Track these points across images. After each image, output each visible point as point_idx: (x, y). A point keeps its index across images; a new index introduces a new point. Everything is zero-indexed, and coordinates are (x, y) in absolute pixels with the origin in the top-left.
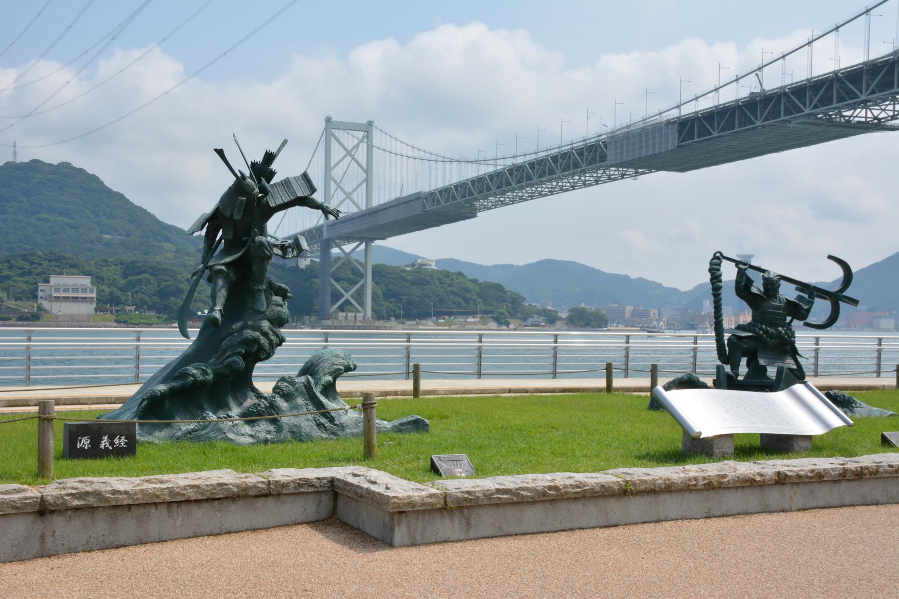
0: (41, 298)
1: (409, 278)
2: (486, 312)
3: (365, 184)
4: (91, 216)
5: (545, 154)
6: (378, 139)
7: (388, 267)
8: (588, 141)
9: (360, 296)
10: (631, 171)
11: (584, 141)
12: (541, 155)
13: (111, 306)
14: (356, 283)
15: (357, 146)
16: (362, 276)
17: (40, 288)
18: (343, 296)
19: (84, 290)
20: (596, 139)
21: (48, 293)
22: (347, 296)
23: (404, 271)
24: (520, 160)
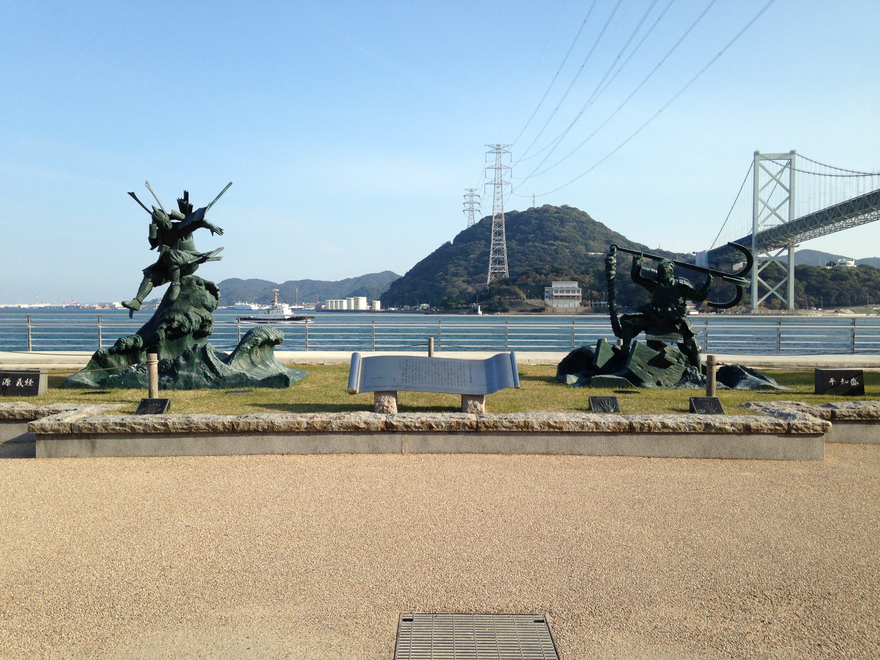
0: (547, 297)
3: (788, 201)
4: (581, 240)
6: (799, 163)
7: (811, 267)
9: (784, 290)
13: (591, 301)
14: (781, 280)
15: (782, 171)
16: (786, 275)
17: (546, 290)
18: (769, 291)
19: (574, 291)
21: (551, 293)
22: (772, 291)
23: (825, 269)
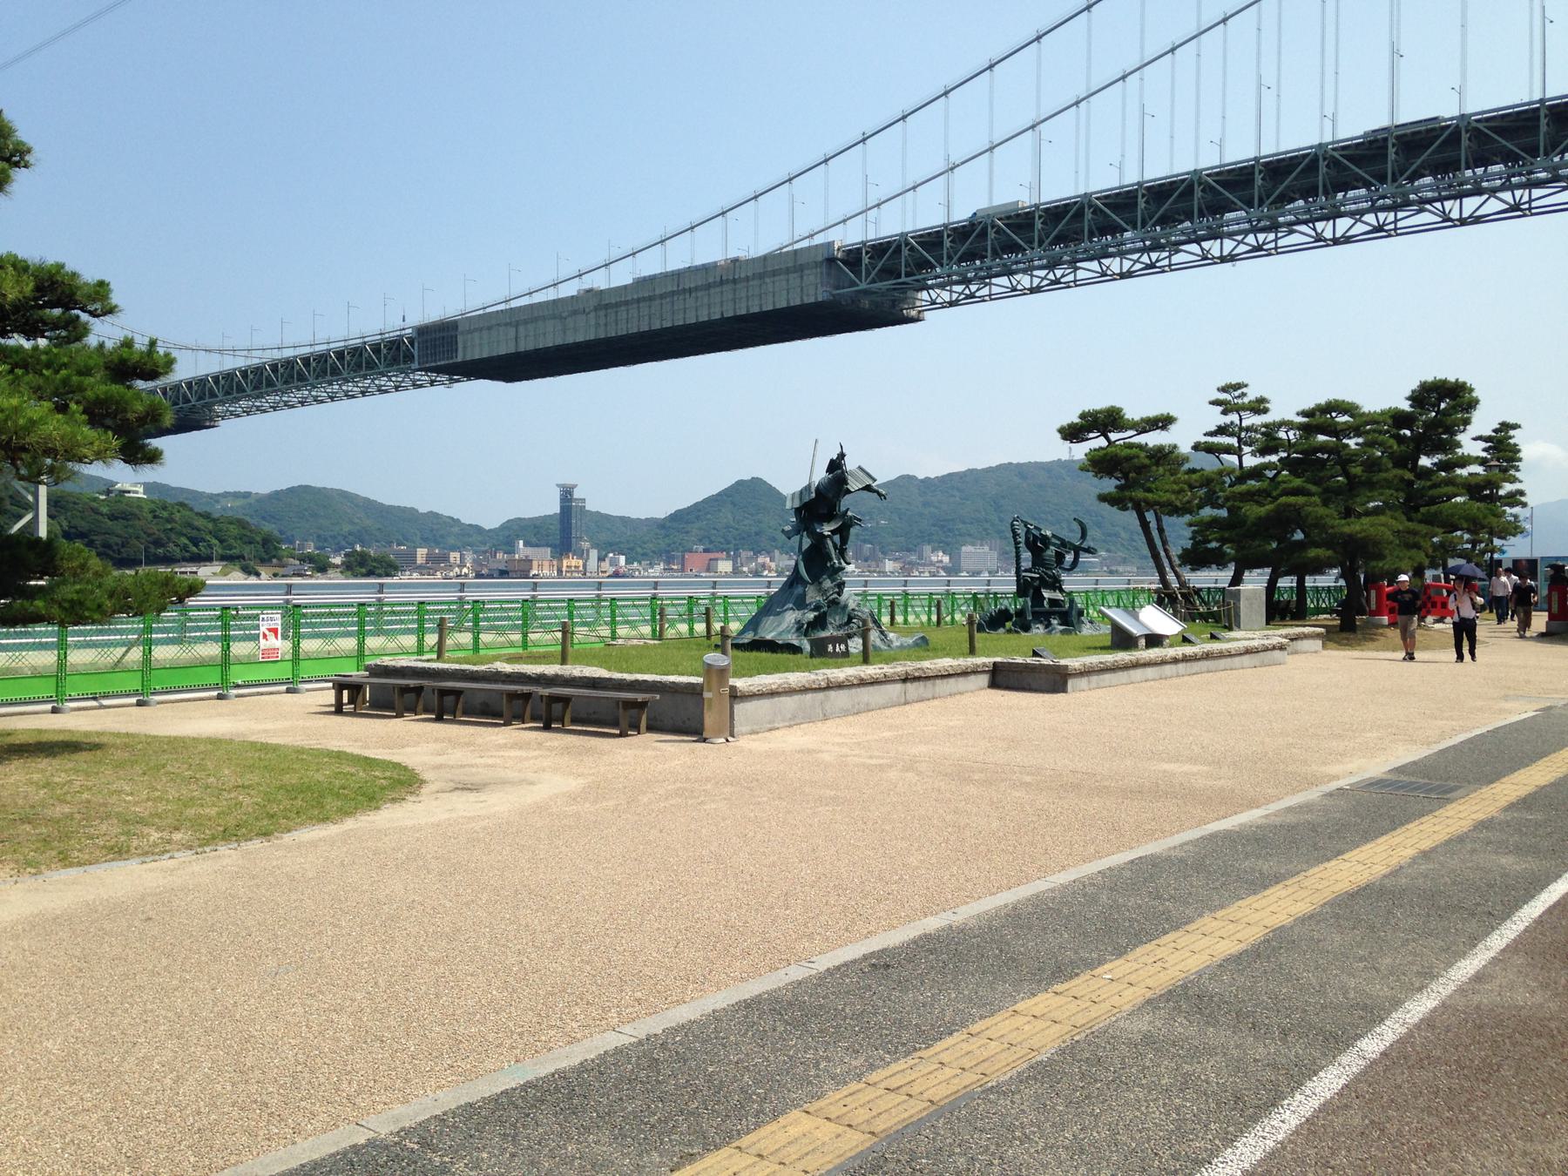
1: (105, 510)
2: (223, 558)
5: (325, 347)
8: (387, 335)
10: (444, 378)
11: (381, 334)
12: (318, 348)
20: (398, 333)
23: (95, 499)
24: (288, 353)
